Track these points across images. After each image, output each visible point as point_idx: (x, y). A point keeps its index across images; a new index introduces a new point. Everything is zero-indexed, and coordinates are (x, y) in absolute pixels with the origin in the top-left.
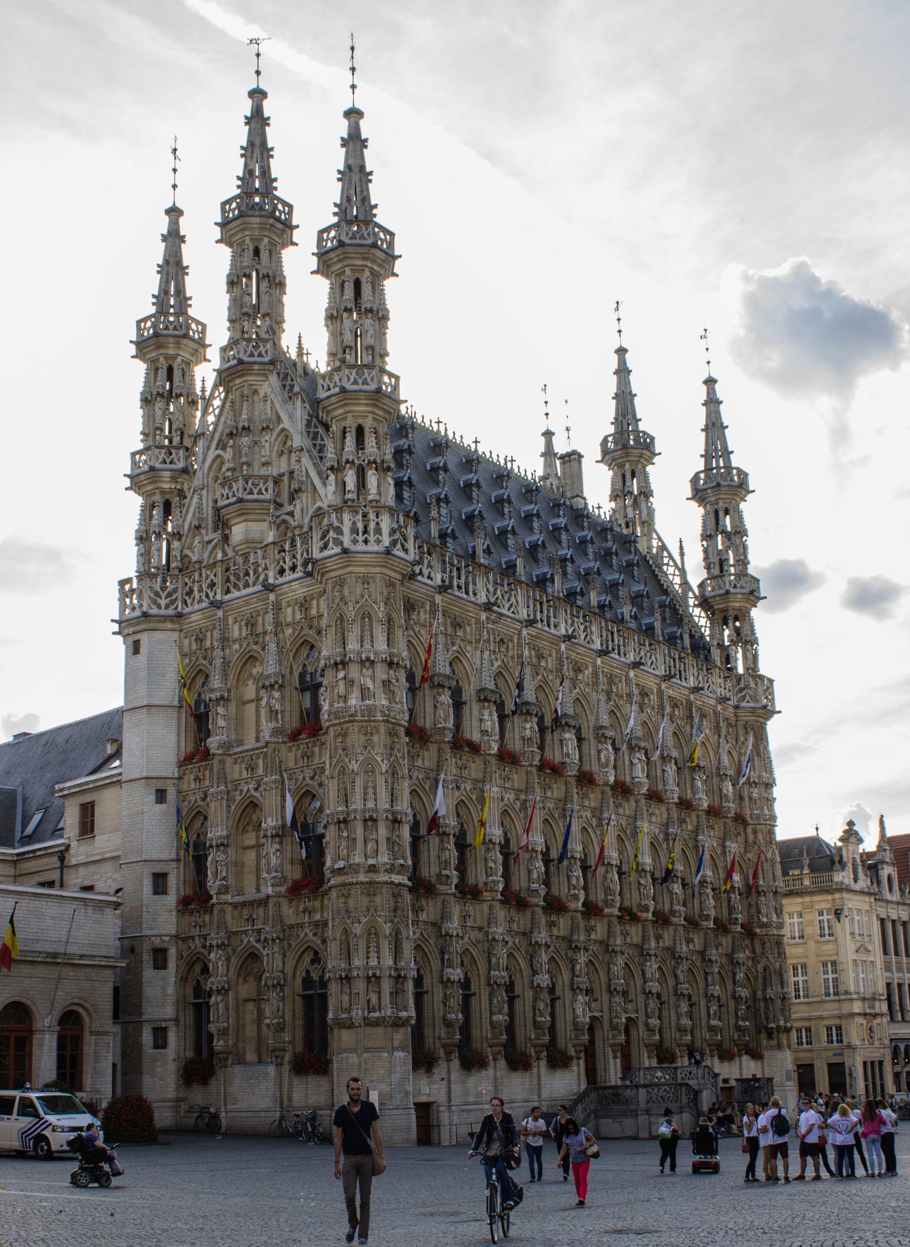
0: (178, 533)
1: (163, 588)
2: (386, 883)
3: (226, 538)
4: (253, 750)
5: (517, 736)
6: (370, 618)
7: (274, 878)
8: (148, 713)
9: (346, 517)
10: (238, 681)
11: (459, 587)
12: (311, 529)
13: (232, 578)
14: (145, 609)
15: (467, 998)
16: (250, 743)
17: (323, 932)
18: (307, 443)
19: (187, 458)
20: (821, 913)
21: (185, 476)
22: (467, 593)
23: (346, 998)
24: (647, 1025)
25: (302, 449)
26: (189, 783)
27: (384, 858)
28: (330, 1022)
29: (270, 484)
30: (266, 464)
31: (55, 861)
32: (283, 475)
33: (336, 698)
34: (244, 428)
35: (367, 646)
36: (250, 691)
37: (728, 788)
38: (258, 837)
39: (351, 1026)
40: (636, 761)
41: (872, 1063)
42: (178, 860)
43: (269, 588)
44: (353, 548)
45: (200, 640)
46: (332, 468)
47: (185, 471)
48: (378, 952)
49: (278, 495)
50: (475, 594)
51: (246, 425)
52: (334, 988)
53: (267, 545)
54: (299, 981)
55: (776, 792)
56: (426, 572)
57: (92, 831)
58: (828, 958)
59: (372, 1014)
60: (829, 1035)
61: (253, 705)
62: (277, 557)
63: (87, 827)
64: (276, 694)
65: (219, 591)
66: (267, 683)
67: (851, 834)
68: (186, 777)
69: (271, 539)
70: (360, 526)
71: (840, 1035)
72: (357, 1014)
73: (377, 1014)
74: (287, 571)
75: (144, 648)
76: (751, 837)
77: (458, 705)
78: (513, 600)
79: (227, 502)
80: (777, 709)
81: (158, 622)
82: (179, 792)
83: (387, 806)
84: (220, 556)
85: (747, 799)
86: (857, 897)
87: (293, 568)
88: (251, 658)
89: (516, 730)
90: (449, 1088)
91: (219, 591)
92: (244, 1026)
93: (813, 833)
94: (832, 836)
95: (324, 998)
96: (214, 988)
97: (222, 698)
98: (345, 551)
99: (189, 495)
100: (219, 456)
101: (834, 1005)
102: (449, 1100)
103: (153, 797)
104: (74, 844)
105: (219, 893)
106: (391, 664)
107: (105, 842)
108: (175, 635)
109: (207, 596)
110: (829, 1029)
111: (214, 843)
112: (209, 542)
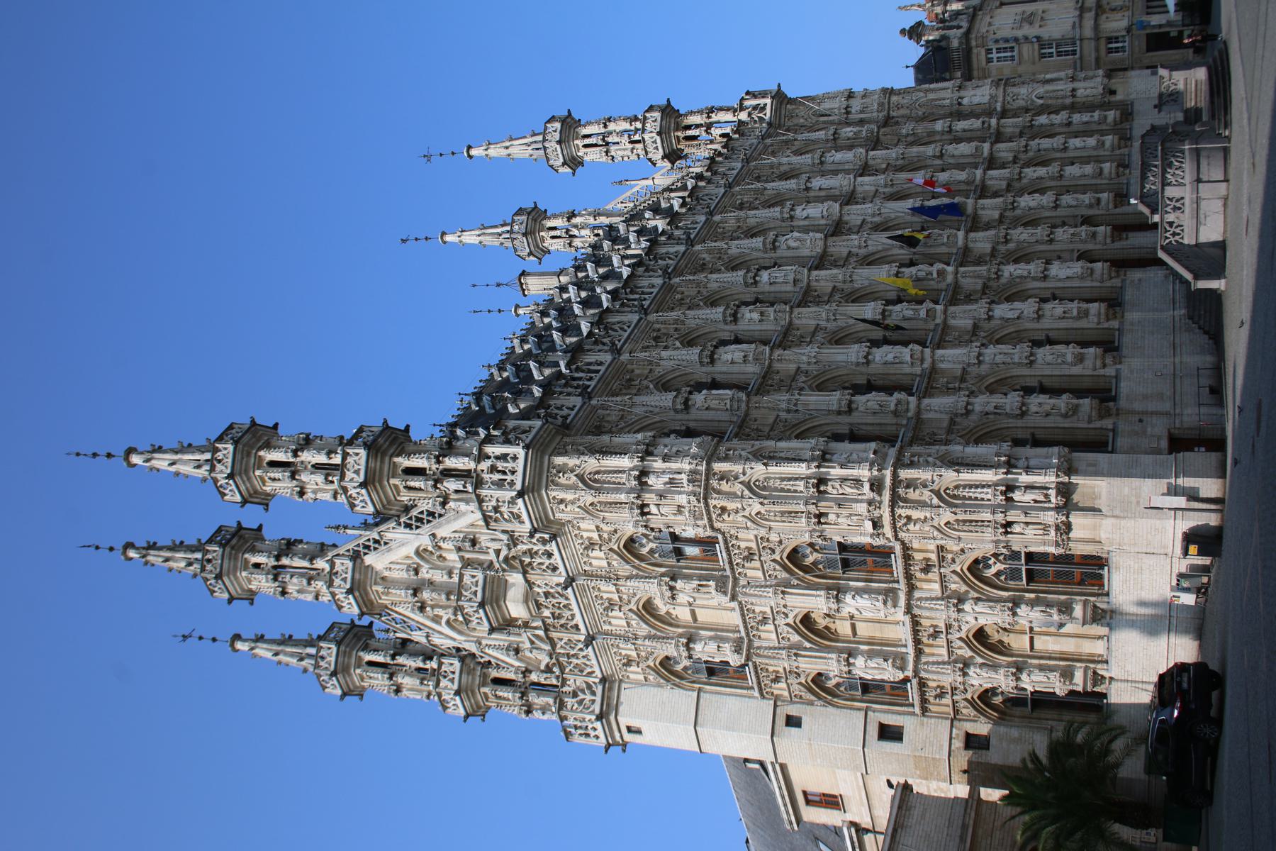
0: (523, 673)
1: (575, 695)
3: (526, 625)
4: (743, 615)
5: (758, 327)
6: (598, 472)
7: (885, 603)
8: (702, 726)
9: (483, 492)
10: (671, 625)
11: (591, 379)
12: (504, 532)
13: (562, 621)
14: (593, 717)
15: (1043, 390)
16: (734, 619)
17: (951, 552)
18: (426, 529)
19: (451, 656)
20: (989, 60)
21: (468, 660)
22: (598, 371)
23: (1030, 531)
24: (1091, 206)
25: (434, 535)
26: (781, 688)
28: (1060, 551)
29: (468, 573)
30: (450, 574)
31: (868, 838)
32: (462, 558)
33: (679, 518)
34: (415, 595)
35: (623, 478)
36: (683, 614)
37: (848, 131)
38: (842, 619)
40: (805, 214)
41: (1148, 7)
42: (866, 711)
43: (570, 581)
44: (518, 486)
45: (629, 663)
46: (444, 504)
47: (462, 660)
48: (977, 487)
49: (480, 564)
50: (601, 364)
51: (410, 592)
52: (1017, 544)
53: (527, 581)
54: (1012, 584)
55: (858, 88)
56: (565, 412)
57: (835, 797)
58: (1036, 53)
59: (1053, 500)
60: (1117, 50)
62: (539, 571)
63: (831, 802)
64: (679, 584)
65: (576, 637)
66: (668, 594)
67: (914, 32)
68: (776, 692)
69: (520, 576)
70: (497, 477)
71: (1117, 39)
72: (1050, 518)
73: (1052, 493)
74: (552, 561)
75: (635, 723)
76: (902, 112)
77: (715, 385)
78: (616, 327)
79: (484, 619)
80: (776, 88)
81: (608, 705)
82: (792, 702)
83: (804, 465)
84: (541, 633)
85: (862, 116)
86: (977, 26)
87: (549, 555)
88: (648, 607)
89: (752, 328)
90: (1152, 413)
91: (576, 637)
92: (1062, 653)
93: (912, 70)
94: (915, 52)
95: (1030, 557)
96: (1013, 684)
97: (687, 645)
98: (521, 494)
99: (487, 659)
100: (448, 622)
101: (1086, 43)
102: (1167, 413)
103: (793, 730)
104: (850, 817)
105: (902, 669)
106: (648, 453)
107: (845, 783)
108: (624, 685)
109: (581, 650)
110: (1110, 51)
111: (846, 669)
112: (532, 642)
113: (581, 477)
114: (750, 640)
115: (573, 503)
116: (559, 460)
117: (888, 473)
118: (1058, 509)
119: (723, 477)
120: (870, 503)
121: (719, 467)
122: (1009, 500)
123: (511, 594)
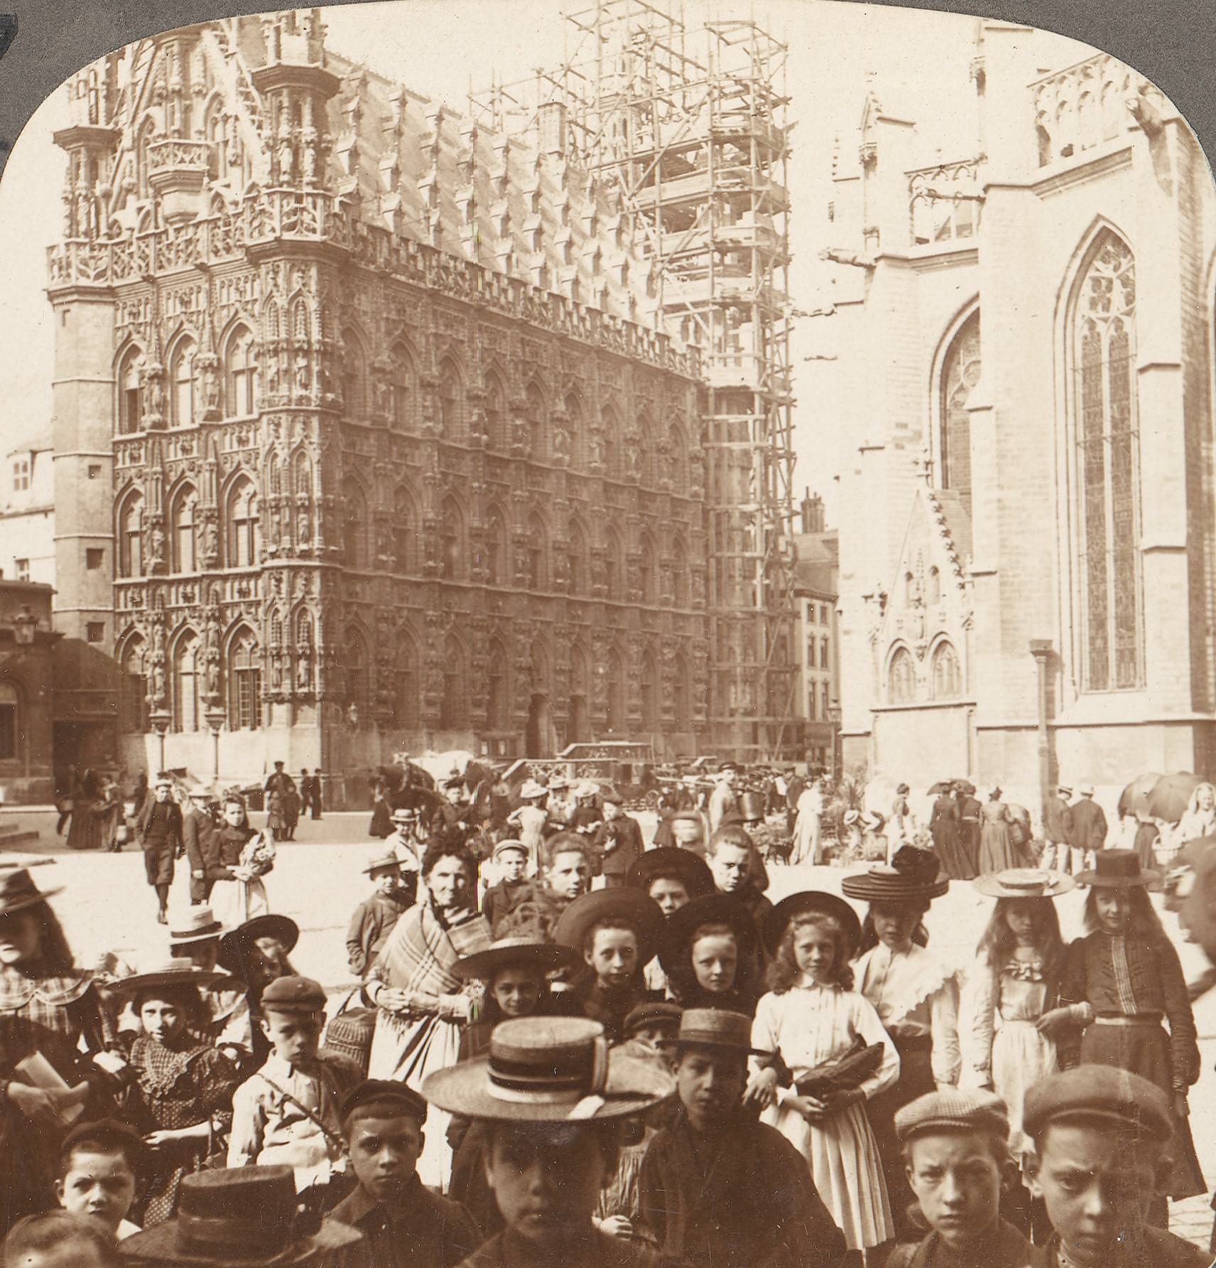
2: (316, 568)
26: (124, 462)
27: (317, 542)
39: (281, 702)
43: (203, 268)
61: (188, 386)
72: (286, 689)
73: (305, 690)
84: (151, 230)
105: (155, 571)
108: (109, 310)
113: (299, 293)
114: (165, 435)
115: (276, 285)
116: (313, 272)
117: (316, 563)
118: (293, 694)
119: (306, 425)
120: (291, 550)
121: (315, 422)
122: (300, 657)
123: (185, 196)
